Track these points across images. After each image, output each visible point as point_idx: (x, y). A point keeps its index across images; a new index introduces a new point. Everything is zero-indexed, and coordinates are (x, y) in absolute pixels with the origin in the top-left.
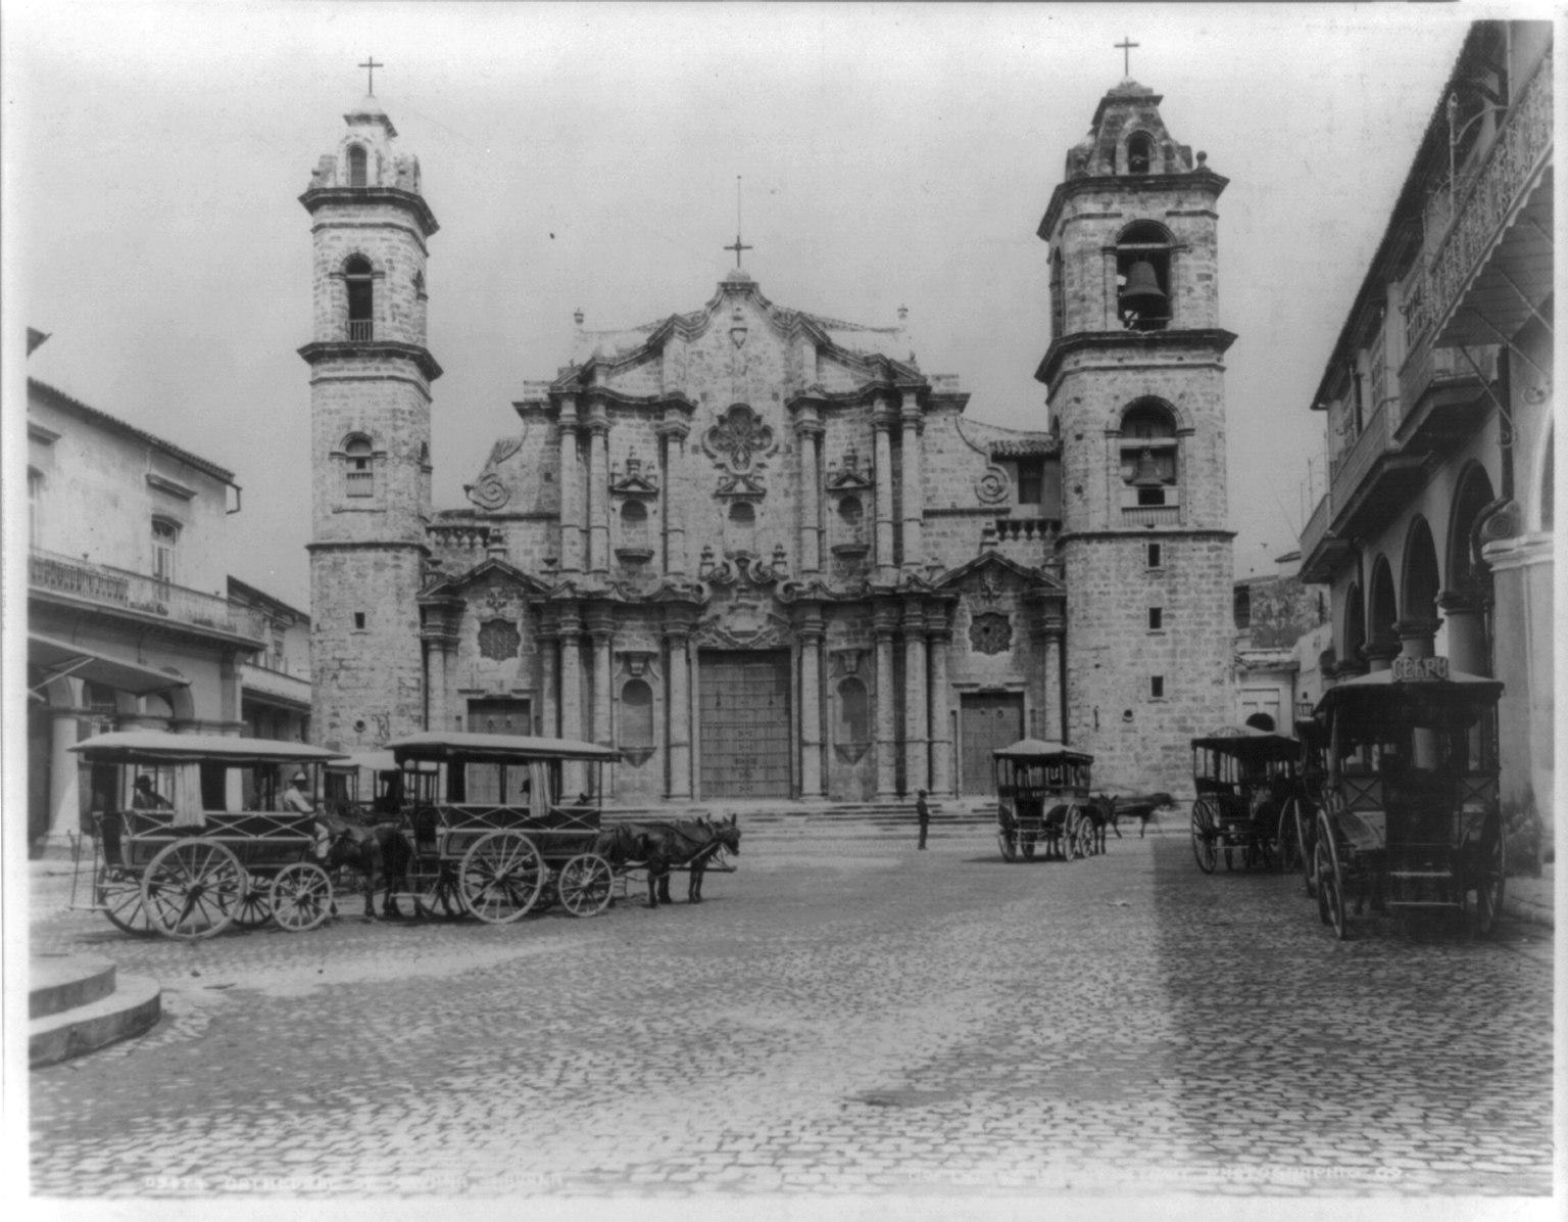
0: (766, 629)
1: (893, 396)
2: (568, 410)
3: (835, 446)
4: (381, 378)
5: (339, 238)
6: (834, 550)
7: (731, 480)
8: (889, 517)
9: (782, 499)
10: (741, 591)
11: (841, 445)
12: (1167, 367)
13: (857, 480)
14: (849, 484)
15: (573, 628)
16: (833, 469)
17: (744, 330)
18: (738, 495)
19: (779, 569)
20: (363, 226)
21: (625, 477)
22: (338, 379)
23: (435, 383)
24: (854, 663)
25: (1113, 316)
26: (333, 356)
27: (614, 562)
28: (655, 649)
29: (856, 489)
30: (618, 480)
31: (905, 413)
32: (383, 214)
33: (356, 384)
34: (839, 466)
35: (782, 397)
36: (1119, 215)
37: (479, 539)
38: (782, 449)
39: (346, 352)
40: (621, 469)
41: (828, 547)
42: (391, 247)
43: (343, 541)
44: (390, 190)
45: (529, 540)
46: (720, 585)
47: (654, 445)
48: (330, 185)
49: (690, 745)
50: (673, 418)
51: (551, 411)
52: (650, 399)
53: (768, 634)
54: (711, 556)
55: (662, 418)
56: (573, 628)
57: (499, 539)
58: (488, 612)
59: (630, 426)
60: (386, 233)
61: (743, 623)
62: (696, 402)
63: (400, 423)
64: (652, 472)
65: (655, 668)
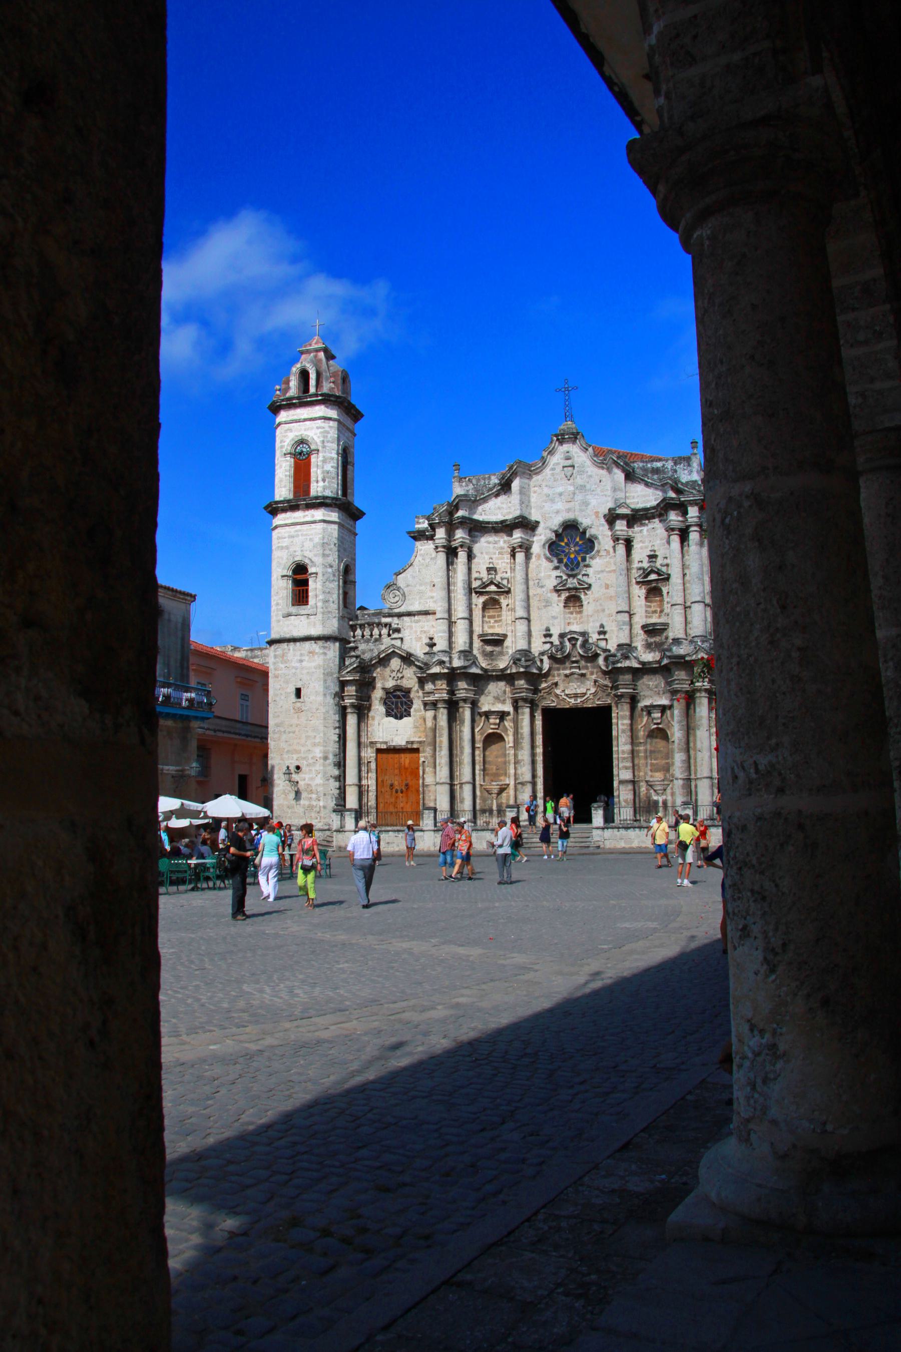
0: (593, 690)
1: (682, 508)
2: (441, 533)
3: (641, 548)
4: (314, 522)
5: (291, 430)
6: (643, 627)
8: (680, 600)
9: (604, 590)
10: (574, 662)
13: (658, 573)
14: (653, 577)
15: (445, 696)
16: (640, 565)
17: (573, 466)
18: (569, 589)
19: (602, 644)
20: (305, 420)
21: (484, 580)
22: (286, 525)
23: (358, 522)
24: (659, 715)
26: (284, 510)
27: (477, 644)
28: (508, 707)
32: (320, 410)
33: (298, 527)
34: (645, 565)
35: (601, 516)
37: (385, 631)
38: (602, 553)
39: (292, 506)
42: (321, 433)
43: (288, 636)
44: (322, 395)
45: (419, 630)
46: (559, 659)
47: (507, 557)
48: (288, 395)
49: (534, 784)
50: (518, 535)
51: (431, 538)
52: (502, 522)
53: (595, 694)
54: (550, 636)
55: (511, 536)
56: (445, 696)
57: (398, 630)
58: (390, 684)
59: (489, 543)
60: (319, 423)
61: (574, 687)
62: (538, 523)
63: (327, 552)
64: (505, 575)
65: (508, 724)
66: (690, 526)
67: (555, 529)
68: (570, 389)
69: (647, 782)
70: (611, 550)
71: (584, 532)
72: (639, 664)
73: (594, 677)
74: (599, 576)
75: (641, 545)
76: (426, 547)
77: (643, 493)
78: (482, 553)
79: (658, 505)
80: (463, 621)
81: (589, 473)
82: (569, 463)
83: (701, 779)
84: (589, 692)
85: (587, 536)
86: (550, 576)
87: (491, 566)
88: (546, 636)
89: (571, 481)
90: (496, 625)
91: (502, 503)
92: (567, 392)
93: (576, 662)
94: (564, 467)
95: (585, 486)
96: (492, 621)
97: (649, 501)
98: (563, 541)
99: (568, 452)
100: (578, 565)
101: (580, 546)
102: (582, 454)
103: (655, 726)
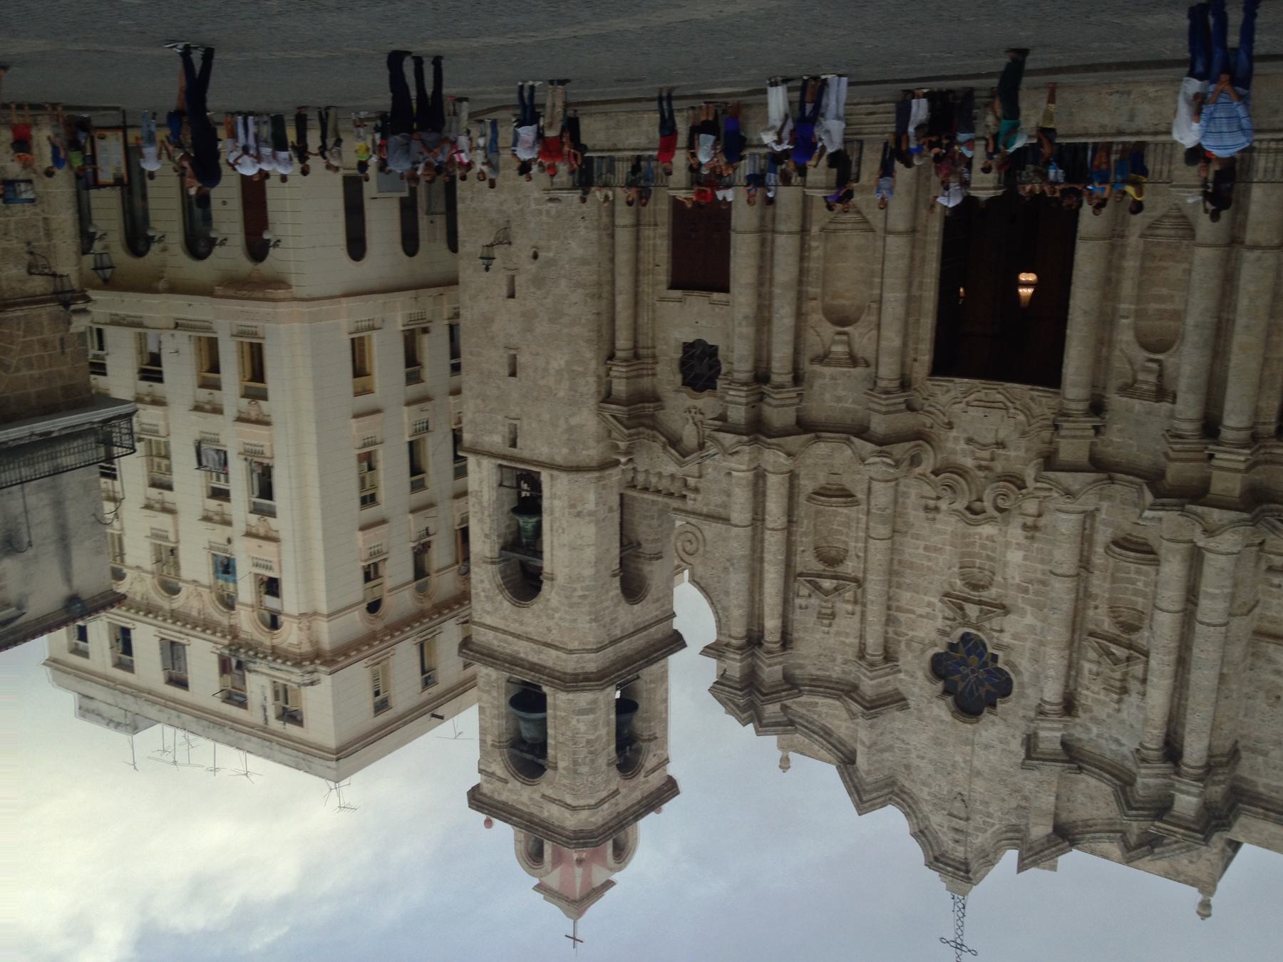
3: (847, 635)
6: (857, 503)
7: (987, 625)
11: (838, 633)
12: (505, 632)
14: (827, 584)
18: (980, 603)
19: (928, 491)
25: (549, 700)
28: (1116, 401)
29: (819, 576)
30: (1138, 669)
31: (738, 657)
36: (544, 796)
40: (1134, 686)
41: (864, 507)
54: (1025, 527)
59: (1117, 741)
64: (1095, 668)
66: (740, 648)
67: (992, 717)
68: (953, 944)
69: (872, 230)
70: (903, 646)
71: (946, 692)
72: (852, 443)
73: (954, 433)
74: (928, 610)
75: (848, 641)
76: (1275, 784)
77: (837, 722)
78: (1132, 726)
79: (800, 693)
80: (1164, 605)
81: (926, 790)
82: (961, 824)
83: (745, 232)
84: (962, 405)
85: (940, 685)
86: (1015, 637)
87: (1115, 697)
88: (1035, 528)
89: (958, 789)
90: (1133, 576)
91: (1082, 804)
92: (959, 941)
93: (980, 468)
94: (967, 819)
95: (936, 771)
96: (1140, 585)
97: (829, 706)
98: (988, 692)
99: (957, 841)
100: (965, 638)
101: (959, 672)
102: (937, 828)
103: (846, 329)
